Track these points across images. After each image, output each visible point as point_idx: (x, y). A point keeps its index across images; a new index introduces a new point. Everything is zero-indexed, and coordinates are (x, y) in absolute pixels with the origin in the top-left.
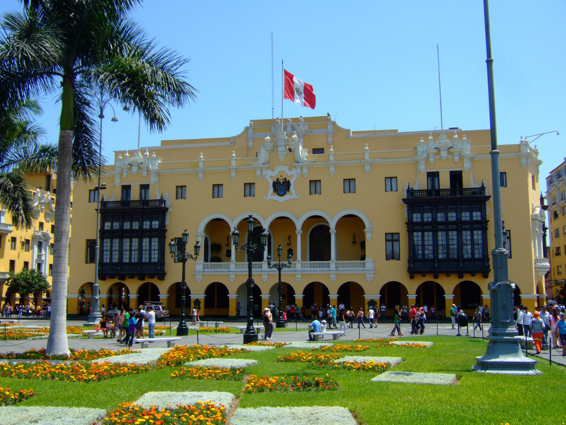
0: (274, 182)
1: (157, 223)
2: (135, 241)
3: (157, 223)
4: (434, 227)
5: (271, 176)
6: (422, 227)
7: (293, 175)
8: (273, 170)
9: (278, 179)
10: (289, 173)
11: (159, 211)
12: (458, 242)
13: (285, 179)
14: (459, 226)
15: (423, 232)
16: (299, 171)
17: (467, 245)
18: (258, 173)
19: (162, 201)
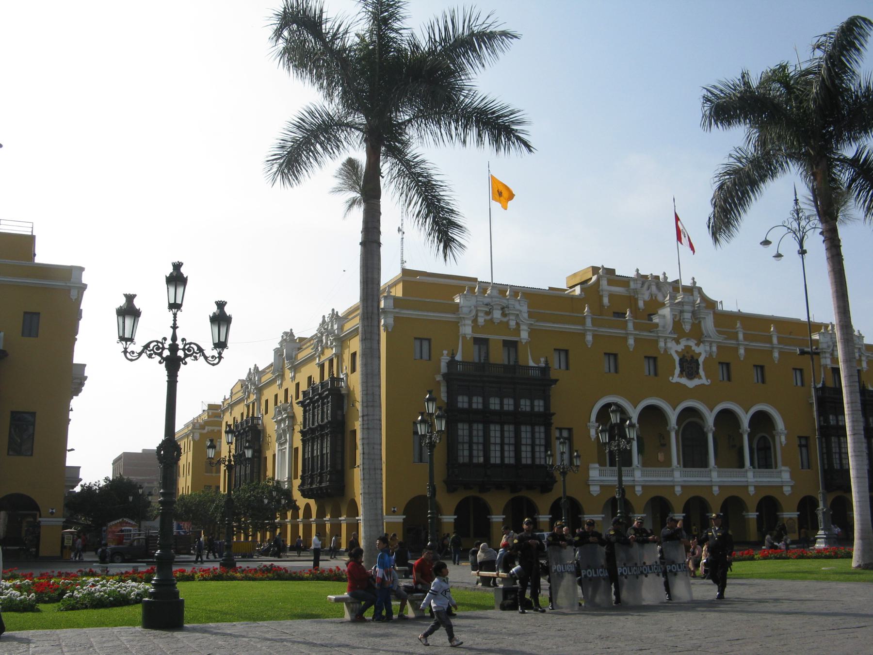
0: (681, 360)
1: (460, 398)
2: (478, 428)
3: (460, 398)
4: (486, 417)
5: (675, 349)
6: (470, 416)
7: (702, 351)
8: (678, 343)
9: (684, 356)
10: (697, 350)
11: (542, 383)
12: (484, 440)
13: (692, 357)
14: (517, 418)
15: (502, 425)
16: (708, 348)
17: (463, 443)
18: (662, 344)
19: (545, 370)
